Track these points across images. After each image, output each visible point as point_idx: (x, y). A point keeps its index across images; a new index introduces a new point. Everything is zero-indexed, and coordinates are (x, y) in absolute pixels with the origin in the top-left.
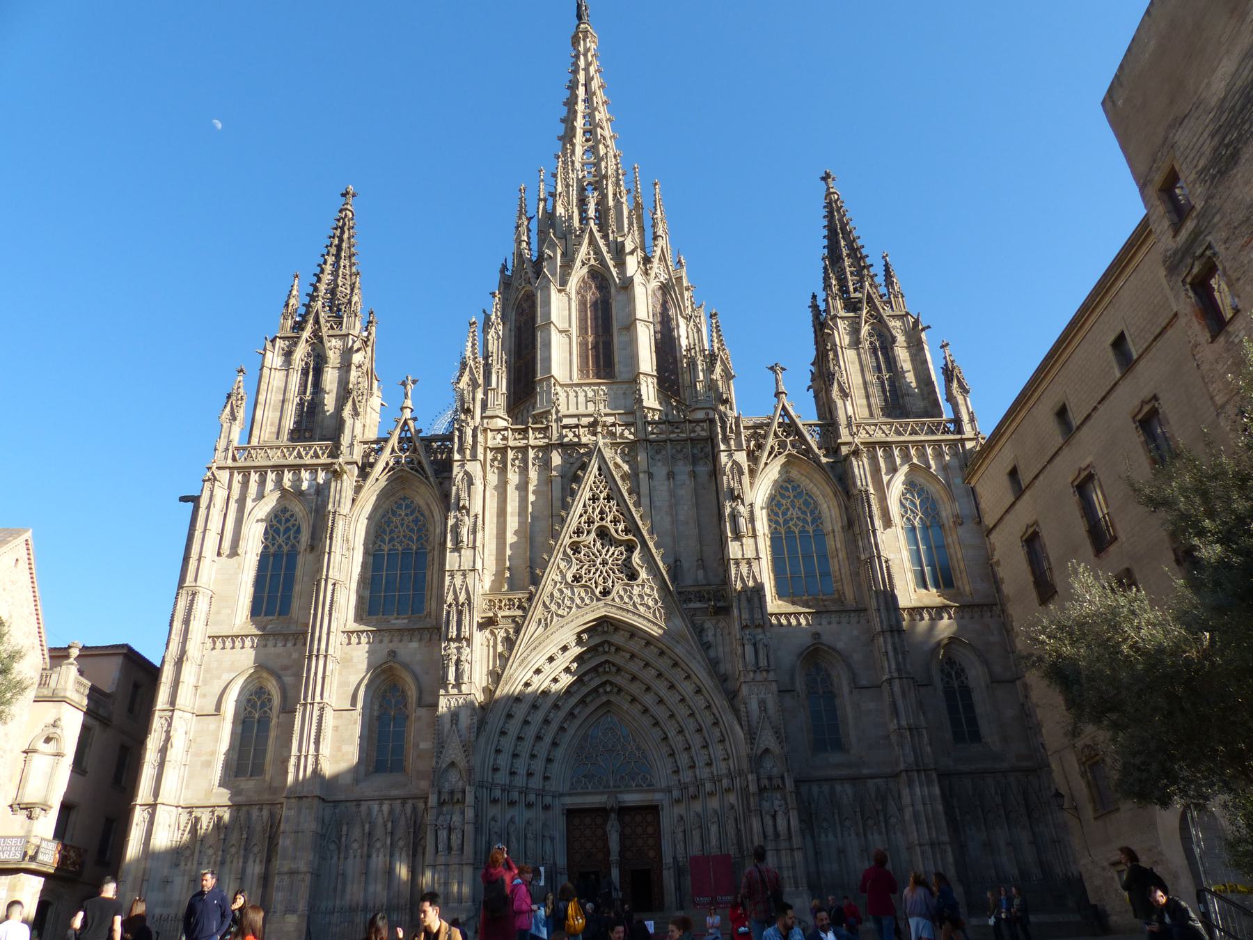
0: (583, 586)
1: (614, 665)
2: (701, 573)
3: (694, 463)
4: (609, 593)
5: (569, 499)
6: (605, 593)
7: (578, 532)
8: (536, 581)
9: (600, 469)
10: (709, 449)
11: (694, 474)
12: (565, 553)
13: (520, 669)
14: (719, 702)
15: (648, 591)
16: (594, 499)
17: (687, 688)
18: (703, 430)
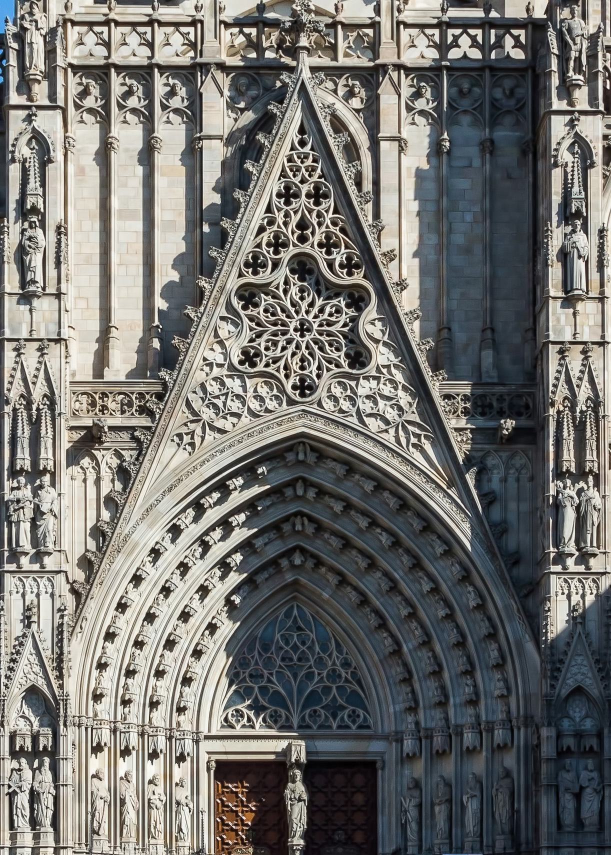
0: (261, 374)
1: (311, 519)
2: (488, 357)
3: (494, 122)
4: (312, 388)
5: (238, 194)
6: (305, 387)
7: (255, 264)
8: (169, 359)
9: (302, 131)
10: (525, 92)
11: (489, 147)
12: (229, 306)
13: (143, 527)
14: (501, 599)
15: (387, 390)
16: (288, 195)
17: (445, 573)
18: (518, 44)
